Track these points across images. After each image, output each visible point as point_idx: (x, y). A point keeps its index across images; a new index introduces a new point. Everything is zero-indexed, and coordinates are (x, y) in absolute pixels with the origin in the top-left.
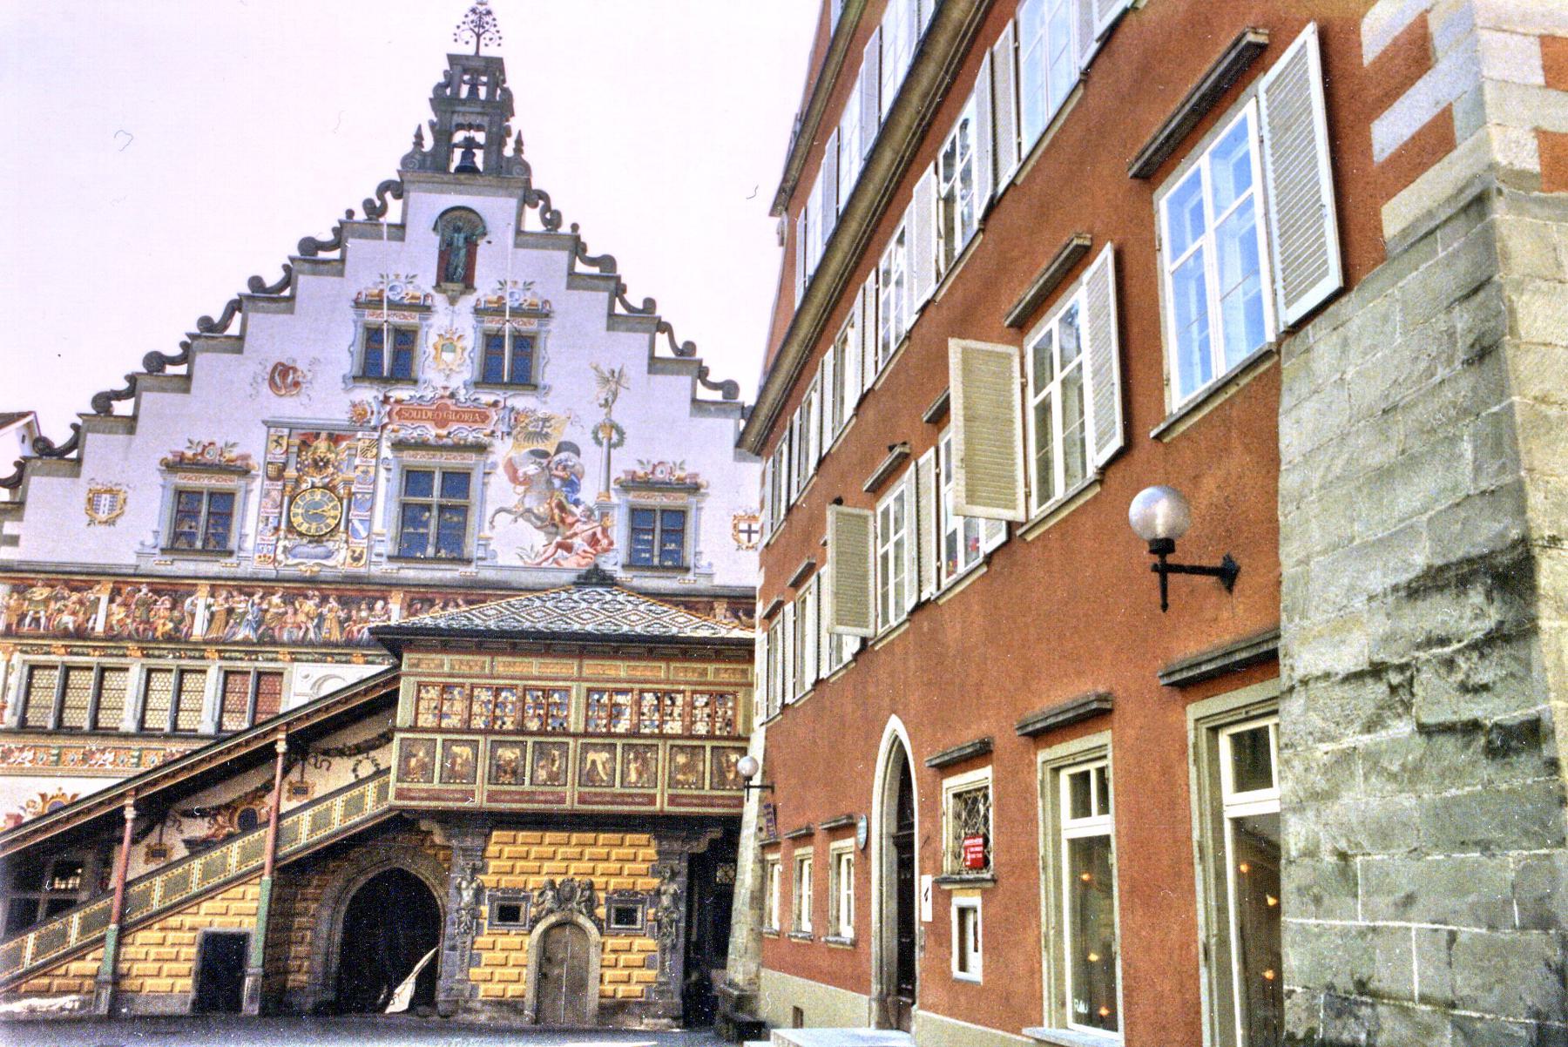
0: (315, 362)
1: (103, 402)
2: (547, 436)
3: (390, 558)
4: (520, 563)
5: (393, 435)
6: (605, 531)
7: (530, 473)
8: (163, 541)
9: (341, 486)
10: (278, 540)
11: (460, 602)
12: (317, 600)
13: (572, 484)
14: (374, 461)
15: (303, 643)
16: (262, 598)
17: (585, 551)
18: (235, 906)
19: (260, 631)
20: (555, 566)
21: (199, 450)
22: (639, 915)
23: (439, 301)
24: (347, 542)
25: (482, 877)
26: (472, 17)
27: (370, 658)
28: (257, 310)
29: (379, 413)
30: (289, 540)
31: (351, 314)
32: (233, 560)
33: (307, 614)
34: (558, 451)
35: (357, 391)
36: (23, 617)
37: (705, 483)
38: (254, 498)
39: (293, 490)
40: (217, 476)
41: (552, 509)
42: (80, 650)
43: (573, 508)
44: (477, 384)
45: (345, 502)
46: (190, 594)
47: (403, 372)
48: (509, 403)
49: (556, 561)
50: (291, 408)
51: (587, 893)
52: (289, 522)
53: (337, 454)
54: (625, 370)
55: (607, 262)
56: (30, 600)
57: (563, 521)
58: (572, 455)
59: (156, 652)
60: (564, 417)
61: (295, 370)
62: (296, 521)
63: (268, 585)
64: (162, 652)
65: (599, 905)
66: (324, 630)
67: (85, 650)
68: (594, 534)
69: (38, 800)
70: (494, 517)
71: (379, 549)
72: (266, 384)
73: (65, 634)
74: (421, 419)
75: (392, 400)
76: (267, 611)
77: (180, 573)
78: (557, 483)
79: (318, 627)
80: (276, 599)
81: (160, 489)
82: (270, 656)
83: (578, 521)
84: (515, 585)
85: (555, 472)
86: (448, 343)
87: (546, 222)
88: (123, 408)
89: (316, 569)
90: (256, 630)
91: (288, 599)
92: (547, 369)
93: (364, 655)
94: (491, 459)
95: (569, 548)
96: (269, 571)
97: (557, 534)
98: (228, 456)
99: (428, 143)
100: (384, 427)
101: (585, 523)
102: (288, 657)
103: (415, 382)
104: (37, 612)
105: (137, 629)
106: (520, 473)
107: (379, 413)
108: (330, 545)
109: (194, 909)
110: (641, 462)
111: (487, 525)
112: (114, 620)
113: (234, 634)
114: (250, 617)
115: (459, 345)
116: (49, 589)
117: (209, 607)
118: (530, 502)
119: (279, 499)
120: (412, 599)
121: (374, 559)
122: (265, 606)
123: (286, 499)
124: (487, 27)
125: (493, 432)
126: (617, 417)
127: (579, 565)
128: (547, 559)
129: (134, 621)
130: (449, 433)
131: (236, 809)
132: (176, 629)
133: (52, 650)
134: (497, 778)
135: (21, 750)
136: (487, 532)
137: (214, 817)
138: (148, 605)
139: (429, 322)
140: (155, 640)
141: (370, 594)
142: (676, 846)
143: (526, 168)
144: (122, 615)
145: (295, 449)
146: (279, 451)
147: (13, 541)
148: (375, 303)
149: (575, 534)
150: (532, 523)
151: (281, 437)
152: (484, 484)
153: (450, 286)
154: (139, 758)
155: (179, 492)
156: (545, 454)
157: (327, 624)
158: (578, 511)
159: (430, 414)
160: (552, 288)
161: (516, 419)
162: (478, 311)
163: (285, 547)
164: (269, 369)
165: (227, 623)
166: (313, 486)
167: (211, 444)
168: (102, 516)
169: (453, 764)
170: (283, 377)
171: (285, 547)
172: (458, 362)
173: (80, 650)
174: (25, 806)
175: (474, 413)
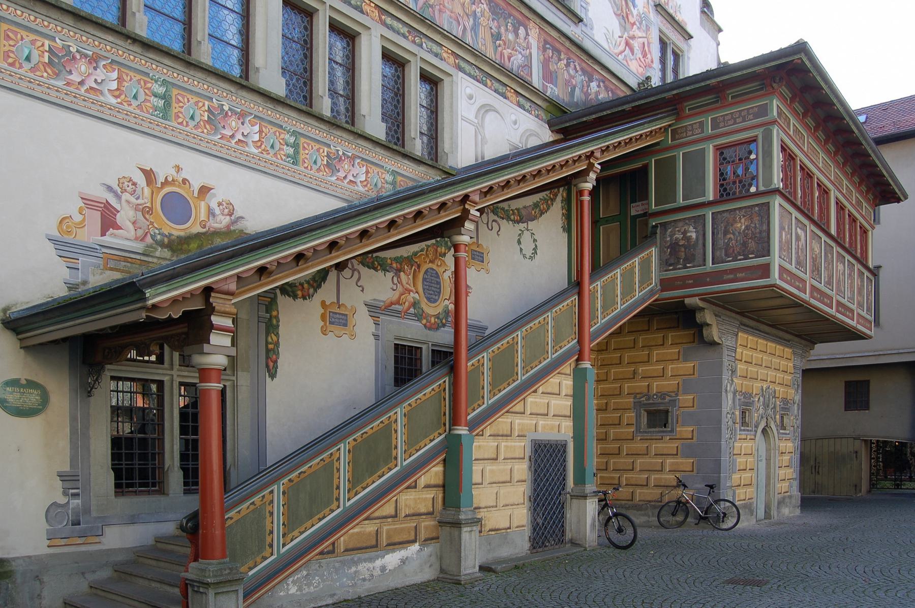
69: (141, 180)
82: (435, 48)
131: (419, 266)
137: (398, 271)
174: (116, 187)
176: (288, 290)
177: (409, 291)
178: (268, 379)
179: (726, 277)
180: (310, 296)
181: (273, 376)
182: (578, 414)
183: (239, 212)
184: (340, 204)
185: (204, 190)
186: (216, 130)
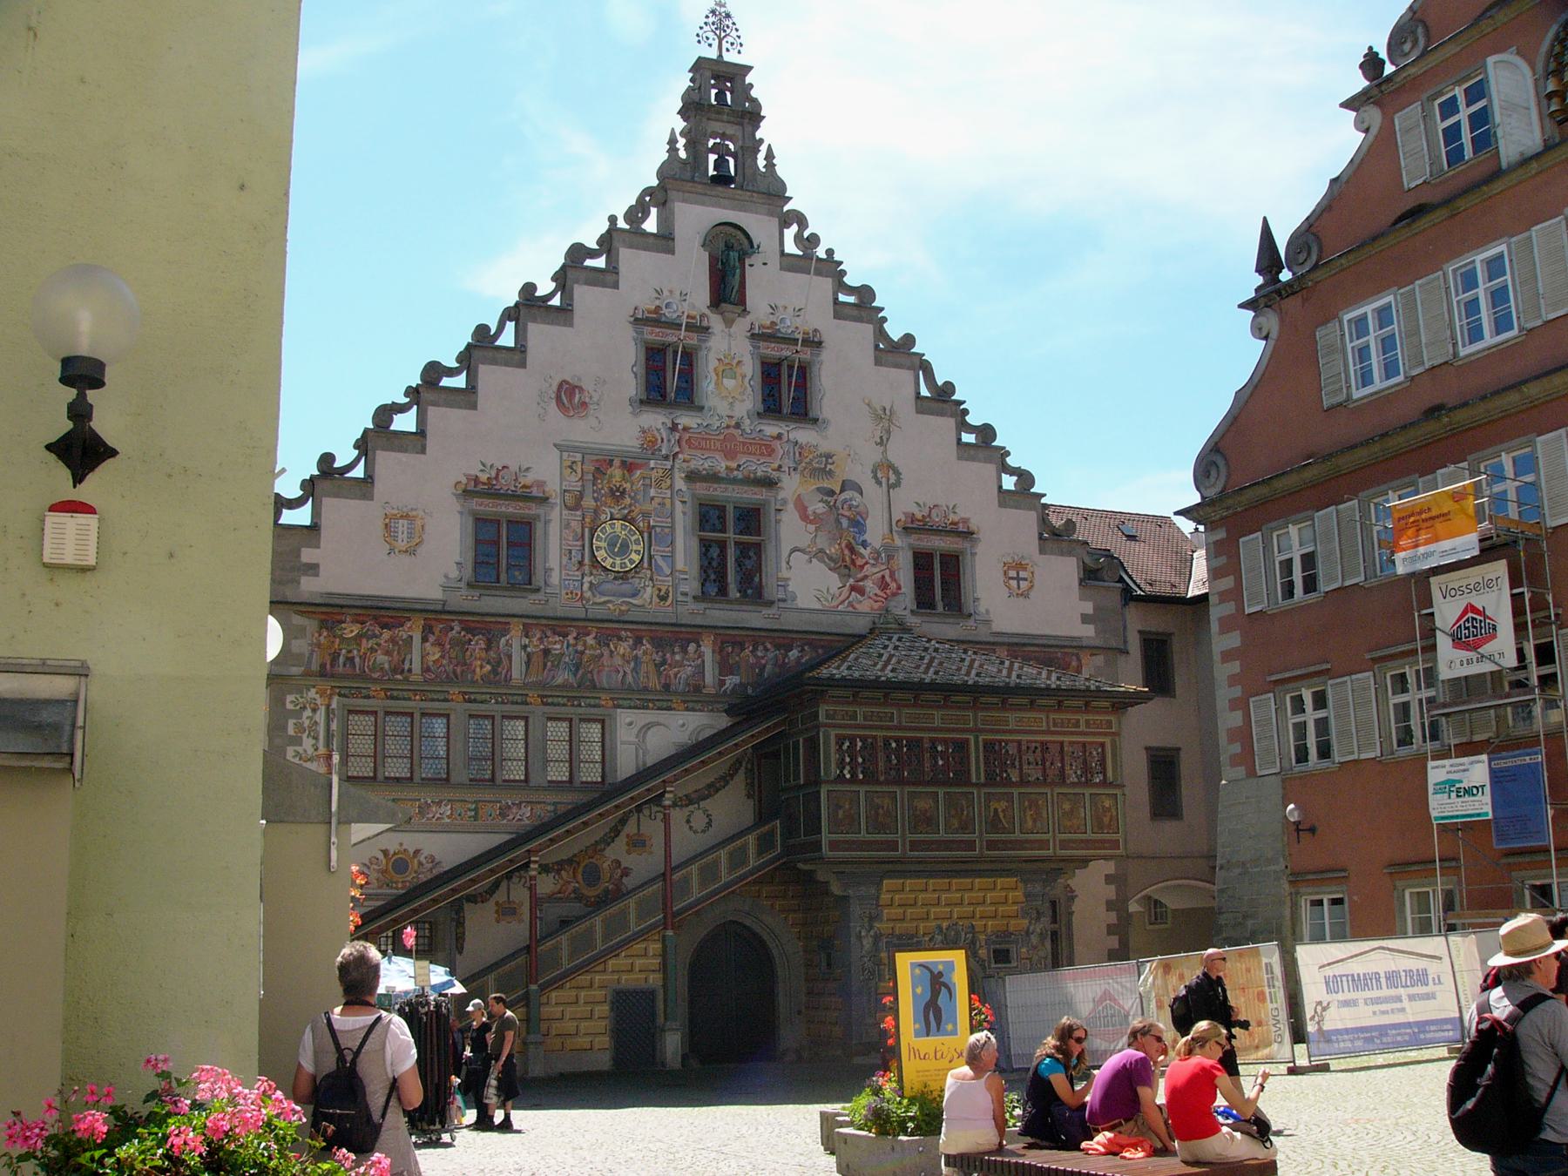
2: (830, 473)
4: (821, 608)
5: (685, 465)
7: (818, 511)
8: (468, 573)
9: (640, 518)
10: (583, 576)
11: (769, 646)
12: (631, 641)
13: (858, 524)
14: (669, 492)
16: (575, 638)
17: (876, 595)
18: (639, 962)
19: (579, 676)
20: (850, 609)
21: (493, 475)
22: (1013, 955)
23: (715, 322)
24: (651, 579)
25: (877, 925)
27: (691, 705)
28: (534, 320)
29: (669, 441)
30: (595, 576)
31: (629, 332)
32: (540, 596)
34: (842, 491)
36: (335, 657)
38: (554, 529)
39: (593, 521)
41: (842, 551)
43: (862, 550)
45: (646, 535)
46: (505, 632)
47: (687, 396)
48: (792, 436)
49: (851, 605)
50: (581, 431)
51: (969, 936)
53: (632, 484)
54: (895, 408)
55: (865, 293)
56: (343, 639)
57: (853, 562)
58: (856, 495)
61: (581, 389)
62: (600, 555)
64: (484, 697)
65: (981, 946)
66: (642, 673)
67: (405, 694)
69: (381, 856)
70: (790, 556)
71: (685, 588)
72: (554, 403)
74: (710, 449)
75: (680, 427)
76: (582, 653)
78: (845, 523)
79: (635, 670)
80: (590, 640)
81: (458, 516)
82: (592, 702)
83: (867, 563)
85: (841, 511)
88: (405, 422)
90: (575, 676)
93: (684, 702)
94: (781, 495)
95: (861, 591)
97: (849, 576)
98: (523, 481)
99: (683, 154)
104: (350, 652)
105: (454, 672)
106: (810, 511)
107: (669, 441)
109: (601, 967)
110: (917, 503)
111: (784, 565)
113: (553, 677)
114: (567, 659)
116: (359, 625)
117: (525, 647)
119: (579, 531)
120: (722, 643)
121: (680, 598)
122: (580, 648)
123: (587, 530)
125: (780, 467)
126: (893, 457)
127: (872, 609)
130: (739, 466)
131: (579, 864)
132: (494, 671)
133: (372, 693)
136: (784, 573)
137: (558, 872)
138: (463, 645)
139: (708, 344)
140: (474, 682)
142: (1038, 888)
144: (437, 656)
145: (591, 477)
146: (574, 478)
149: (866, 577)
152: (778, 522)
153: (730, 307)
155: (480, 521)
156: (831, 493)
157: (644, 668)
159: (718, 444)
160: (818, 318)
161: (800, 453)
162: (756, 337)
163: (591, 583)
164: (555, 388)
165: (545, 665)
167: (504, 467)
168: (402, 544)
170: (569, 396)
171: (591, 583)
175: (761, 445)
176: (472, 899)
177: (569, 882)
178: (458, 956)
180: (487, 900)
181: (460, 953)
182: (664, 967)
183: (438, 858)
184: (507, 837)
185: (417, 852)
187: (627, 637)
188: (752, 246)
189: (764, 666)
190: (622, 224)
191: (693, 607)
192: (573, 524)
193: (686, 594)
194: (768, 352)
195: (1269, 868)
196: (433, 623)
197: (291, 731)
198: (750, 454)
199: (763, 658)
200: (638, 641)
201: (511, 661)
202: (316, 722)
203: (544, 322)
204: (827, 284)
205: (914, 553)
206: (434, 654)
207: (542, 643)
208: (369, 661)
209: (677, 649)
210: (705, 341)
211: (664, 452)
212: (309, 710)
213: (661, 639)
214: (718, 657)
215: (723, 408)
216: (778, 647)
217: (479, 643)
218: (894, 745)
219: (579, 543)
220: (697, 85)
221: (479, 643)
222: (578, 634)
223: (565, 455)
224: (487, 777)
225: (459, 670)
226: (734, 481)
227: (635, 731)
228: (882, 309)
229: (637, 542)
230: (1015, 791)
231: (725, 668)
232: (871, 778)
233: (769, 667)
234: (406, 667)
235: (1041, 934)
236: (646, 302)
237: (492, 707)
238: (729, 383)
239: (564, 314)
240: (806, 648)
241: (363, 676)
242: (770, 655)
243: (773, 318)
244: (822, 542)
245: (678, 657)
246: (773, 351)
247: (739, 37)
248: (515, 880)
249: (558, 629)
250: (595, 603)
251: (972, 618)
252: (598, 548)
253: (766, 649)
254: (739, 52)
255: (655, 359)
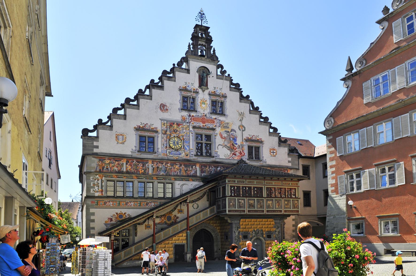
0: (171, 104)
1: (115, 110)
2: (228, 127)
3: (195, 155)
4: (225, 158)
5: (192, 125)
6: (243, 151)
7: (225, 136)
8: (138, 149)
9: (181, 137)
11: (213, 167)
12: (179, 165)
13: (235, 139)
14: (188, 131)
15: (177, 175)
20: (233, 159)
23: (200, 91)
24: (184, 151)
26: (200, 15)
29: (188, 119)
30: (170, 150)
31: (179, 92)
32: (156, 154)
33: (177, 169)
34: (231, 132)
35: (182, 113)
37: (263, 141)
40: (149, 133)
42: (121, 177)
43: (236, 145)
44: (211, 113)
45: (183, 141)
50: (166, 116)
52: (169, 145)
53: (179, 129)
54: (244, 113)
57: (233, 148)
58: (234, 132)
59: (141, 178)
60: (232, 123)
61: (166, 106)
62: (171, 145)
63: (168, 160)
64: (142, 178)
68: (241, 151)
72: (159, 109)
73: (116, 172)
74: (198, 121)
76: (167, 168)
77: (143, 157)
78: (232, 139)
79: (180, 172)
80: (169, 165)
82: (169, 179)
83: (237, 148)
84: (224, 163)
85: (231, 136)
86: (203, 102)
87: (221, 72)
89: (177, 157)
90: (165, 172)
91: (172, 165)
92: (227, 111)
94: (216, 132)
95: (235, 155)
96: (166, 157)
97: (232, 151)
98: (151, 127)
100: (190, 122)
101: (238, 149)
102: (174, 179)
103: (196, 111)
105: (134, 172)
106: (223, 136)
107: (188, 119)
108: (180, 151)
111: (217, 148)
112: (128, 169)
113: (160, 173)
115: (206, 103)
118: (226, 143)
120: (202, 166)
122: (166, 166)
124: (204, 18)
125: (216, 126)
126: (243, 124)
128: (231, 157)
129: (133, 169)
130: (206, 125)
132: (145, 171)
134: (250, 207)
135: (109, 202)
136: (217, 150)
138: (137, 166)
140: (139, 174)
141: (191, 164)
143: (217, 58)
144: (130, 168)
146: (164, 127)
147: (97, 147)
148: (185, 89)
149: (236, 151)
150: (227, 148)
151: (164, 123)
152: (215, 138)
154: (140, 204)
156: (228, 132)
157: (182, 171)
158: (237, 146)
159: (201, 120)
162: (209, 94)
164: (159, 105)
165: (157, 171)
166: (174, 137)
167: (147, 124)
169: (240, 204)
170: (163, 107)
171: (169, 152)
172: (206, 107)
173: (121, 177)
179: (223, 212)
186: (127, 205)
187: (178, 164)
188: (209, 72)
189: (212, 171)
190: (176, 66)
191: (194, 158)
192: (164, 138)
193: (192, 155)
194: (213, 98)
195: (341, 216)
196: (129, 160)
197: (92, 185)
198: (209, 122)
199: (211, 169)
200: (181, 165)
201: (149, 169)
202: (99, 183)
203: (156, 89)
204: (228, 83)
205: (248, 146)
206: (129, 167)
207: (157, 165)
208: (112, 169)
209: (190, 167)
210: (197, 95)
211: (187, 121)
212: (97, 180)
213: (187, 165)
214: (200, 169)
215: (202, 112)
216: (215, 167)
217: (141, 165)
218: (244, 188)
219: (166, 142)
220: (196, 32)
221: (141, 165)
222: (166, 163)
223: (162, 121)
224: (143, 196)
225: (135, 171)
226: (205, 129)
227: (180, 186)
228: (241, 89)
229: (180, 142)
230: (274, 199)
231: (202, 171)
232: (238, 196)
233: (213, 172)
234: (122, 170)
235: (279, 232)
236: (183, 85)
237: (144, 180)
238: (203, 105)
239: (161, 88)
240: (222, 167)
241: (111, 172)
242: (213, 169)
243: (214, 90)
244: (226, 143)
245: (190, 169)
246: (214, 98)
247: (206, 20)
248: (150, 219)
249: (161, 162)
250: (170, 156)
251: (262, 161)
252: (171, 144)
253: (212, 168)
254: (207, 24)
255: (185, 99)
